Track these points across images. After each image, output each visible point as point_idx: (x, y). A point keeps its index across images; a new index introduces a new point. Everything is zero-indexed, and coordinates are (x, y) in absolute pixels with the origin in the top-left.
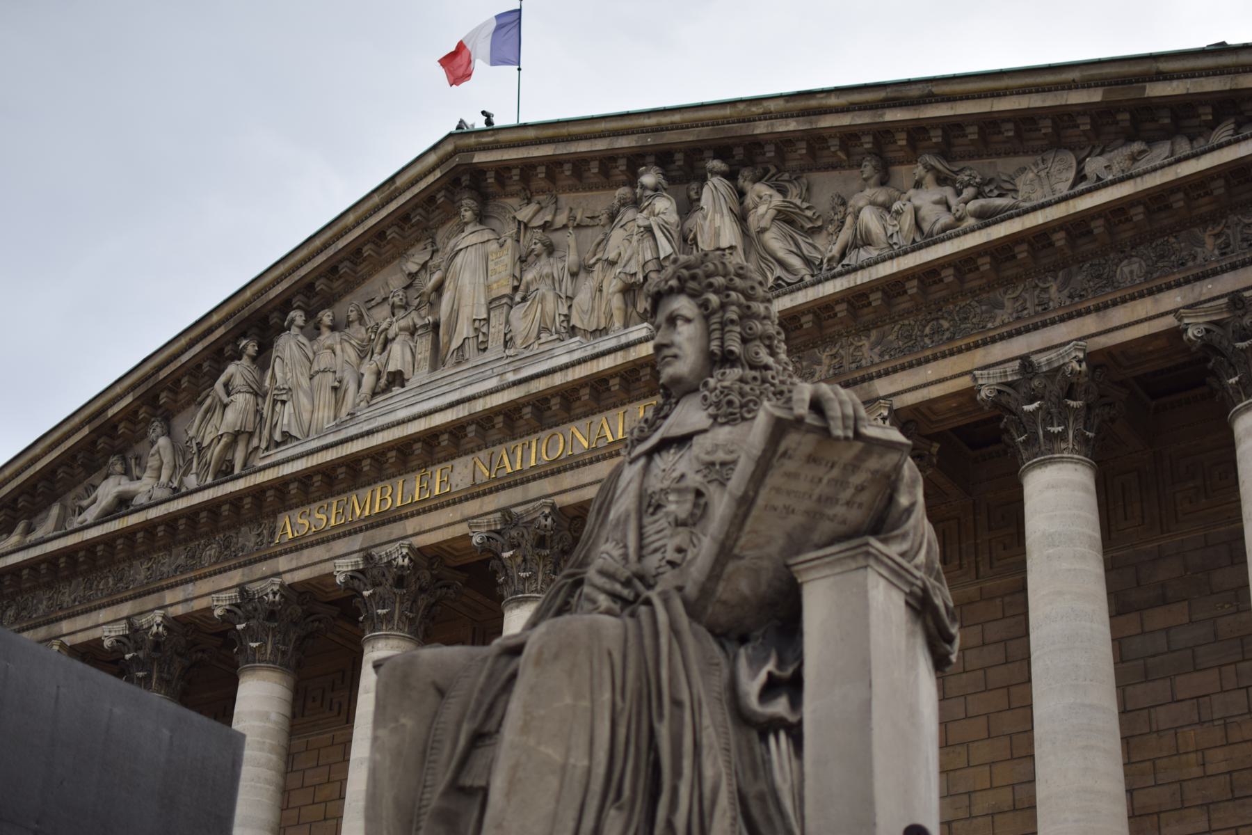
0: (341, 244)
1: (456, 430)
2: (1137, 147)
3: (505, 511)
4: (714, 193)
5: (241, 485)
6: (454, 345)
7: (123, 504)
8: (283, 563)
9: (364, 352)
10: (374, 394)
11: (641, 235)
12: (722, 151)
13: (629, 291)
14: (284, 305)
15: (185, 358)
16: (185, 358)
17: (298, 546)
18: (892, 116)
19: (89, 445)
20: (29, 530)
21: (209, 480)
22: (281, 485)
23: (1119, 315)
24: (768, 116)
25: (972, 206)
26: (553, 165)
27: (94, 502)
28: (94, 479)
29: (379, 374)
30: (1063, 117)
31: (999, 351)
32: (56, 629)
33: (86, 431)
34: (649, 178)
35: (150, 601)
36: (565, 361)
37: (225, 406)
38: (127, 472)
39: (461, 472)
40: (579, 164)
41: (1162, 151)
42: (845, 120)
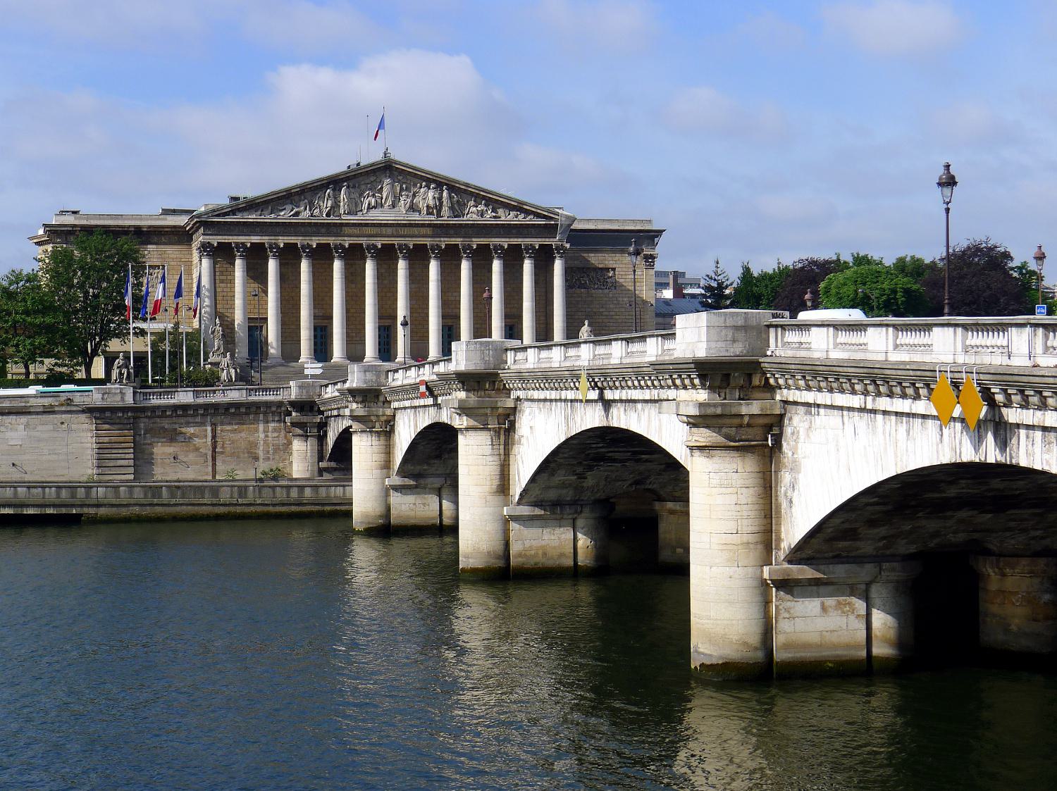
0: (359, 172)
2: (519, 213)
4: (445, 194)
7: (297, 214)
8: (346, 238)
10: (369, 208)
11: (428, 196)
12: (446, 184)
13: (428, 206)
15: (315, 185)
18: (481, 193)
20: (262, 211)
21: (324, 215)
23: (512, 240)
25: (494, 214)
28: (280, 201)
29: (369, 204)
31: (493, 239)
32: (277, 238)
33: (285, 193)
34: (432, 186)
36: (415, 217)
38: (291, 203)
41: (521, 217)
42: (473, 190)
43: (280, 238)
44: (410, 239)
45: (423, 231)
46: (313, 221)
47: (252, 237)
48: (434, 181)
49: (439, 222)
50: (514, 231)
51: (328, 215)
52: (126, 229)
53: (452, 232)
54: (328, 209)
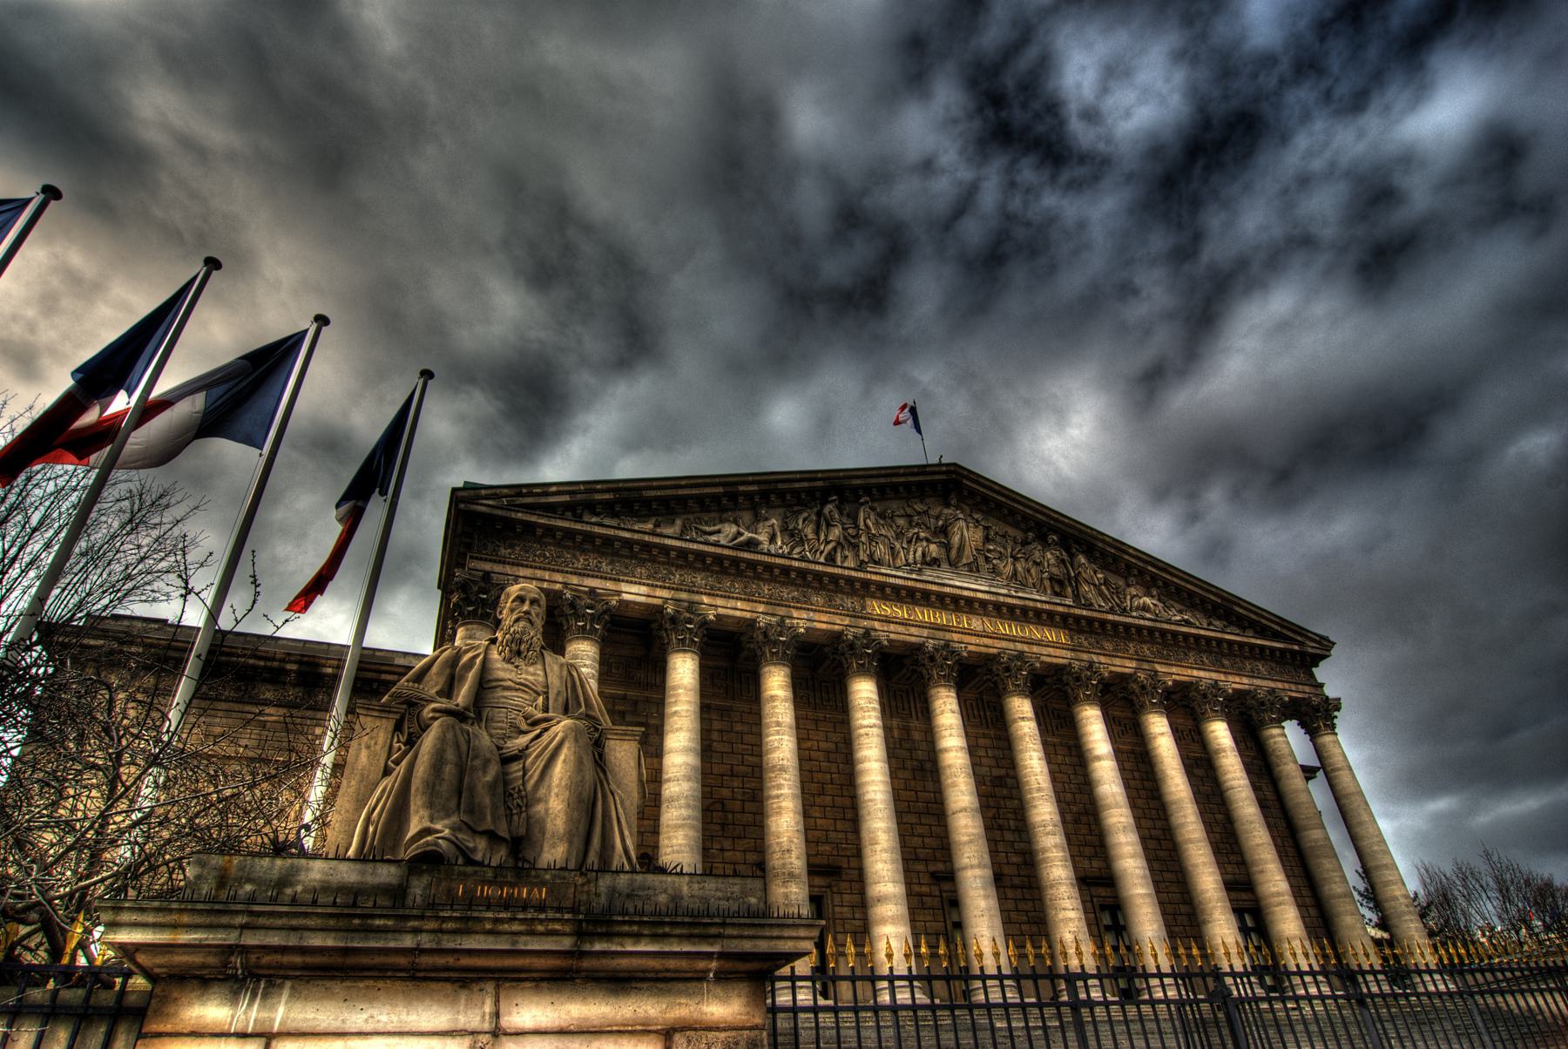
0: (895, 480)
1: (983, 603)
3: (1022, 652)
5: (860, 575)
6: (964, 561)
7: (751, 545)
9: (899, 535)
10: (924, 562)
13: (1051, 579)
14: (855, 490)
15: (797, 485)
16: (797, 485)
17: (887, 620)
19: (716, 498)
21: (822, 560)
22: (881, 587)
24: (1103, 541)
26: (999, 505)
27: (719, 532)
29: (924, 555)
30: (1203, 600)
31: (1195, 673)
32: (696, 598)
33: (721, 490)
35: (782, 611)
37: (829, 525)
38: (736, 522)
39: (976, 623)
40: (1012, 512)
43: (706, 599)
44: (1026, 648)
45: (1050, 635)
46: (796, 564)
47: (624, 587)
48: (1055, 530)
49: (1084, 613)
50: (1226, 662)
51: (831, 560)
52: (276, 664)
53: (1108, 646)
54: (830, 547)
